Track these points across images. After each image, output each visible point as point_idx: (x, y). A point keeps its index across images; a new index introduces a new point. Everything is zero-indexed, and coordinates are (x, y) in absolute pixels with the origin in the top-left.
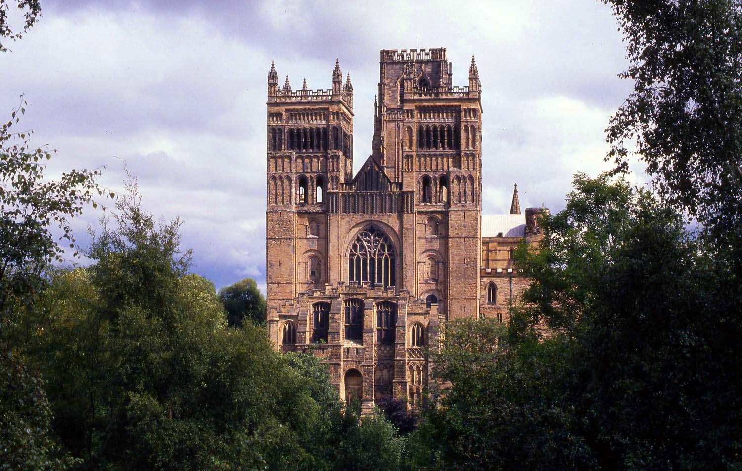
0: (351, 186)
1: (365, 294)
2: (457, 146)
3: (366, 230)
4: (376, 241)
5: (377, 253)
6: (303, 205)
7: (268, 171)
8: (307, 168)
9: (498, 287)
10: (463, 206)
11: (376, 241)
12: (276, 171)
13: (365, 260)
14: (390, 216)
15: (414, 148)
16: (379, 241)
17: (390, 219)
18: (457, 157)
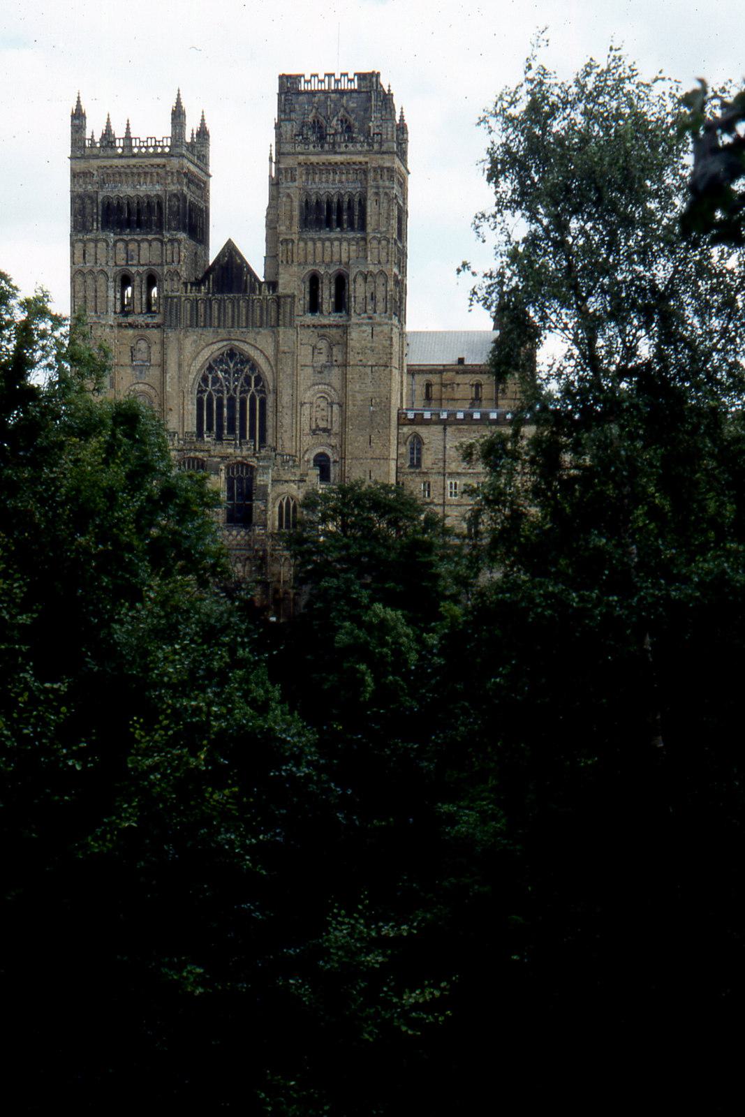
0: (200, 286)
1: (208, 451)
2: (363, 227)
3: (223, 354)
4: (237, 372)
5: (239, 388)
7: (73, 263)
8: (132, 259)
9: (426, 441)
10: (370, 318)
11: (237, 372)
12: (85, 263)
13: (220, 401)
14: (258, 333)
15: (296, 228)
16: (242, 371)
17: (258, 338)
18: (362, 243)
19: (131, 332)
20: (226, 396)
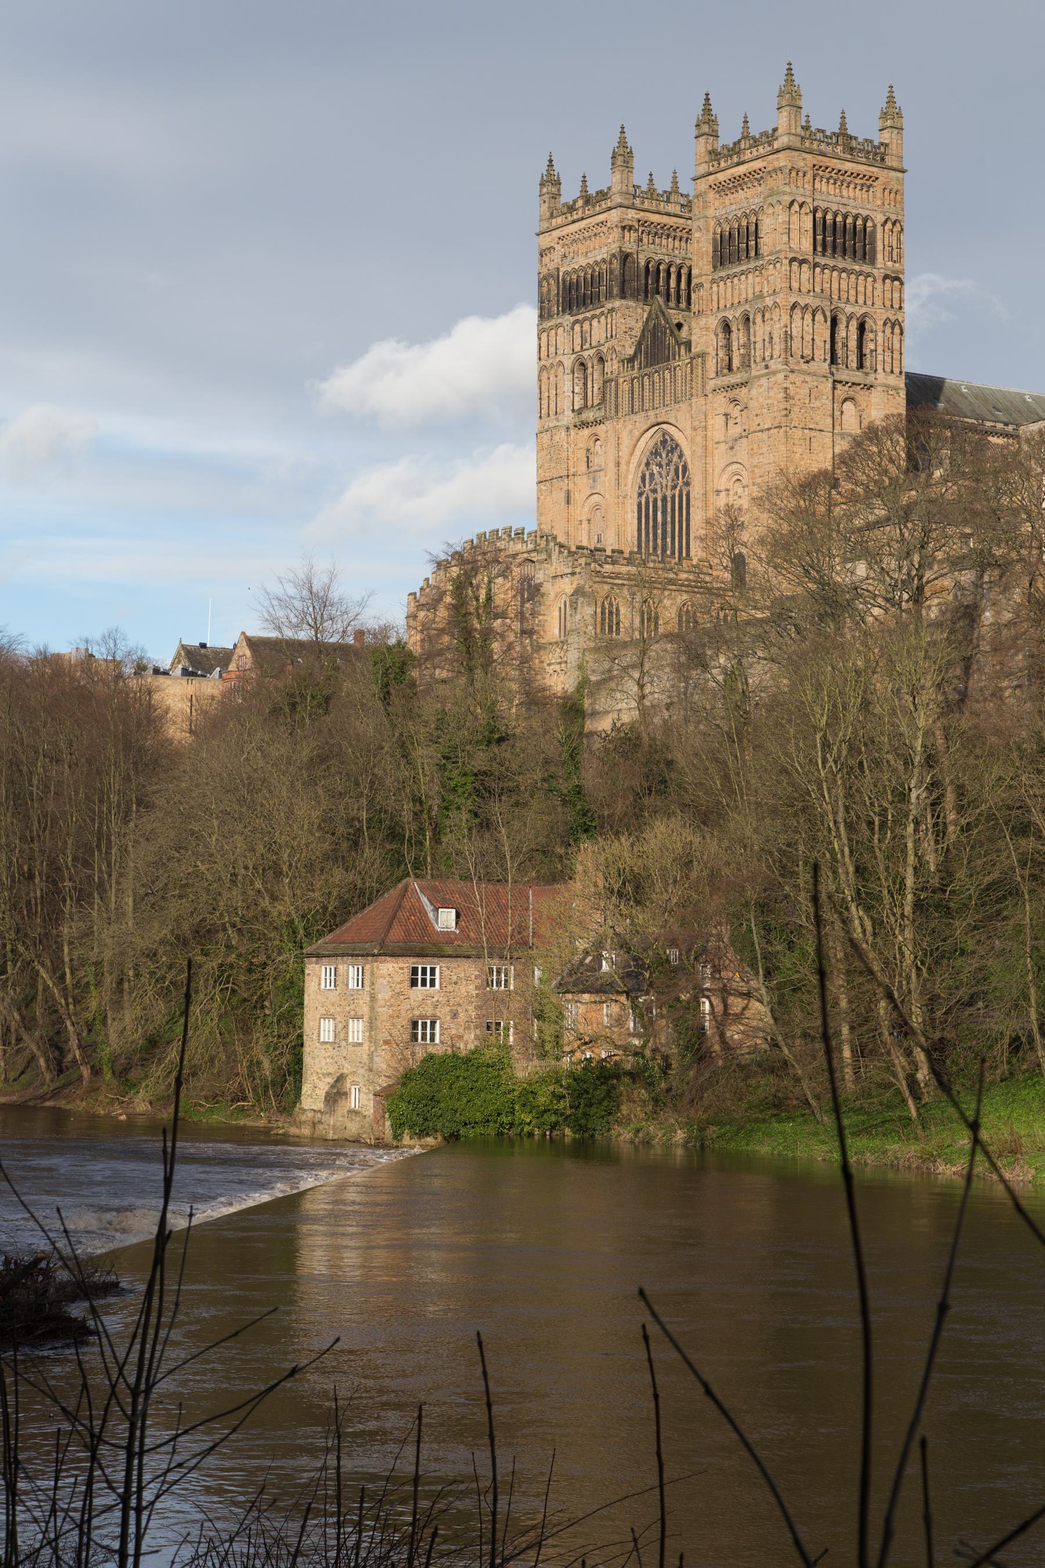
6: (580, 412)
19: (586, 432)
20: (659, 496)
